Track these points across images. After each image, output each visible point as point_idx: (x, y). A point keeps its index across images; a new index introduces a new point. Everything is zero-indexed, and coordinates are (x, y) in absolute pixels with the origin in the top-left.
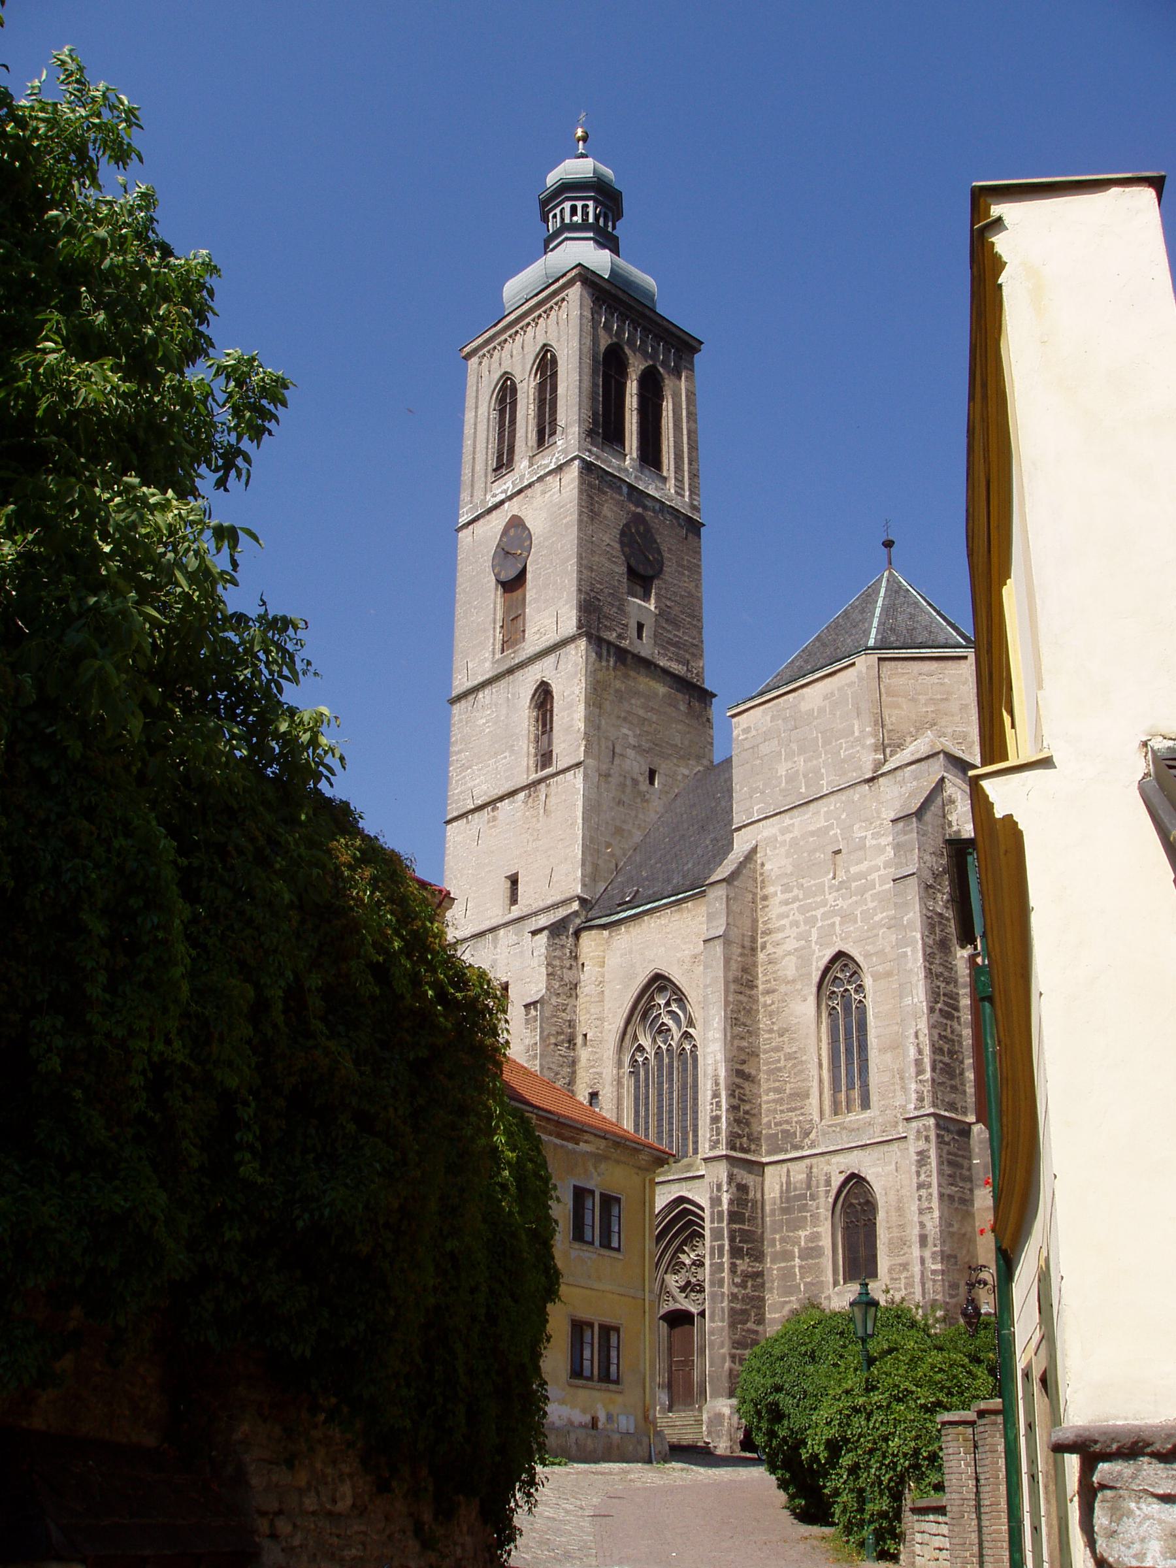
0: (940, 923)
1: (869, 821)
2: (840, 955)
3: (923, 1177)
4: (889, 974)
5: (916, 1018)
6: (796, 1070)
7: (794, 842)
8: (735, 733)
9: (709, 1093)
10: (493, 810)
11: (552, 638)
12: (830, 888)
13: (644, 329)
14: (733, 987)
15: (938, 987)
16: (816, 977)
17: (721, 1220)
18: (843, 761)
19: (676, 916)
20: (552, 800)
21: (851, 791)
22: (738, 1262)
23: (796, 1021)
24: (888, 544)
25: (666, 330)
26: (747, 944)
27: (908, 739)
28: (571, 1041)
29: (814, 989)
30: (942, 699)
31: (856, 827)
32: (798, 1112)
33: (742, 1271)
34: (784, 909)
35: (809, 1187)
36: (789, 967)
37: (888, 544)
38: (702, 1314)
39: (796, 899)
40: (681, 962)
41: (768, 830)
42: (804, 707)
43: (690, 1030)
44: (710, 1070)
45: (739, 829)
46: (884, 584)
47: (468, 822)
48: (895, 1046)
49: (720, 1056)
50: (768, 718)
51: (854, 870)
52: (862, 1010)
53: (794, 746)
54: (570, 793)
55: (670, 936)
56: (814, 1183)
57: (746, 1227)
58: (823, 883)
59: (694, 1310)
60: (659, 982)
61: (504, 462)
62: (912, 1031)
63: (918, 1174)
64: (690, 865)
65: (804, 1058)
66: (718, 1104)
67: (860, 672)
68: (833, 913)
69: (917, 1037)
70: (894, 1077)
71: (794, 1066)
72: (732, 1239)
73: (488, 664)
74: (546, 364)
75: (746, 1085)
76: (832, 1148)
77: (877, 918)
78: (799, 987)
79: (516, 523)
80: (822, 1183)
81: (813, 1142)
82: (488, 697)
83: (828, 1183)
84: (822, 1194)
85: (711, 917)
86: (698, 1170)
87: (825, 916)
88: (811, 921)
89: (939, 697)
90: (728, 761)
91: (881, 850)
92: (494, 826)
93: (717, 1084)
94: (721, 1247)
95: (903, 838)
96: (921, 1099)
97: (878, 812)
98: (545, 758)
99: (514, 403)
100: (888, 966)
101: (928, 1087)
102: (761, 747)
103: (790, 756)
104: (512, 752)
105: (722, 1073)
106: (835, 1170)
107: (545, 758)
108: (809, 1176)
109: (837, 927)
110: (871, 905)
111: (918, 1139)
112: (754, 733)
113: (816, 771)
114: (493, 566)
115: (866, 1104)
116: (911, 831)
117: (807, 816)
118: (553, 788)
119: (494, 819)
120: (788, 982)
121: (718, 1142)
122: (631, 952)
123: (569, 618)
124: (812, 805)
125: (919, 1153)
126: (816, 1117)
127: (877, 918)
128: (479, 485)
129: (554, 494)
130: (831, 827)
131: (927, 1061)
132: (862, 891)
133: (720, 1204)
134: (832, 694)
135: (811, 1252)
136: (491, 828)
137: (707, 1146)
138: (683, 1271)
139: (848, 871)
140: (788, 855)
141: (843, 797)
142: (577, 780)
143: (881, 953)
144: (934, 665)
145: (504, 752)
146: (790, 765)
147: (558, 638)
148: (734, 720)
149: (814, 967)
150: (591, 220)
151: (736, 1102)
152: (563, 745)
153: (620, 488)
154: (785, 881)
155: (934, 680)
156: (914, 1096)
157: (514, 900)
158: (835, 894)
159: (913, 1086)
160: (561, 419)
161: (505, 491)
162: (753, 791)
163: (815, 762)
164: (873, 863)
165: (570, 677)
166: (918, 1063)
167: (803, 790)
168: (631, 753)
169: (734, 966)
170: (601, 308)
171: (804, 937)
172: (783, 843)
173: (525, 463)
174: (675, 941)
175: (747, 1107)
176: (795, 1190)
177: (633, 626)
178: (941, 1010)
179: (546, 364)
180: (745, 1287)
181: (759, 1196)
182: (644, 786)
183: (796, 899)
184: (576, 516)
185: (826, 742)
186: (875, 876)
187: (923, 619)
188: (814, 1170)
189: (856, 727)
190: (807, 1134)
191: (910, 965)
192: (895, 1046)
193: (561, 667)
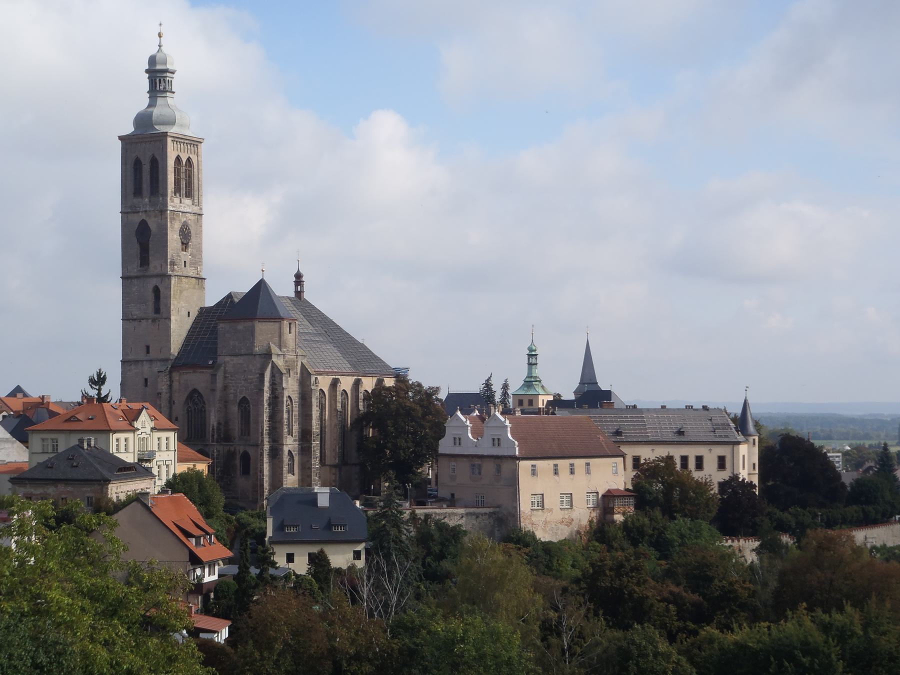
2: (244, 397)
36: (231, 397)
41: (228, 359)
60: (195, 391)
98: (157, 310)
105: (215, 424)
106: (241, 449)
107: (157, 310)
115: (249, 434)
173: (147, 200)
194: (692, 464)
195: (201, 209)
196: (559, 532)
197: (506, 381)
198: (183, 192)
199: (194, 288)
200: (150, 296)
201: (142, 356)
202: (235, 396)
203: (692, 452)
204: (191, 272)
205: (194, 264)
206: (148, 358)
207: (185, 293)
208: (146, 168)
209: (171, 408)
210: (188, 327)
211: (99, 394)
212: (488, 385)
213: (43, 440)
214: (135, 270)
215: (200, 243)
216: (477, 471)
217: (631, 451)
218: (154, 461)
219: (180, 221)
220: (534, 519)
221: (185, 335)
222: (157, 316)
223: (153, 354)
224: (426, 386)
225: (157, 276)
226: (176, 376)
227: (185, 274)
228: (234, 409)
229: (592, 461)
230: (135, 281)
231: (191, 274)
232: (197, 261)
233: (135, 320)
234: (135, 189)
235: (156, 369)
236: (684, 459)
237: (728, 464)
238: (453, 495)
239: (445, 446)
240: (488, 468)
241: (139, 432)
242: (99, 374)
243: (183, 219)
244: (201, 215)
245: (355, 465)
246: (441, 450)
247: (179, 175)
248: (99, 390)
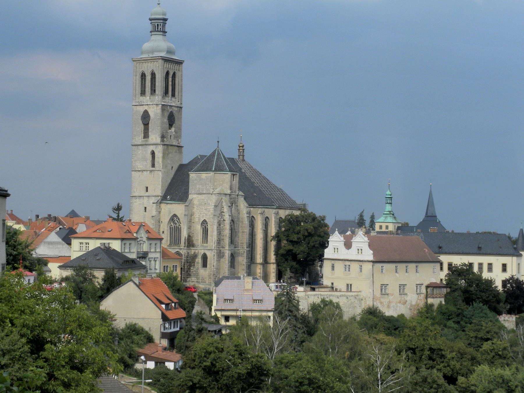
24: (218, 142)
28: (159, 222)
36: (197, 220)
37: (218, 142)
41: (195, 196)
48: (212, 236)
52: (208, 229)
60: (175, 215)
88: (201, 213)
98: (153, 165)
99: (145, 79)
105: (186, 236)
106: (202, 252)
107: (153, 165)
128: (137, 96)
135: (198, 263)
142: (160, 173)
165: (159, 152)
173: (148, 98)
174: (178, 209)
177: (169, 137)
187: (222, 162)
194: (485, 268)
195: (181, 104)
196: (398, 308)
197: (373, 214)
199: (176, 152)
200: (150, 157)
201: (143, 193)
202: (199, 219)
203: (485, 260)
204: (175, 143)
205: (177, 137)
206: (147, 194)
207: (170, 155)
208: (148, 78)
209: (160, 226)
210: (172, 176)
211: (118, 216)
212: (361, 216)
213: (81, 243)
214: (139, 139)
215: (181, 125)
216: (347, 269)
217: (446, 259)
218: (147, 258)
219: (168, 111)
220: (382, 300)
221: (170, 181)
222: (153, 169)
223: (150, 193)
224: (317, 215)
225: (153, 145)
226: (163, 205)
227: (171, 143)
228: (198, 229)
229: (420, 265)
230: (140, 147)
231: (174, 143)
232: (178, 136)
234: (142, 91)
235: (152, 202)
236: (481, 265)
237: (508, 268)
238: (332, 284)
239: (328, 253)
240: (355, 267)
241: (139, 240)
242: (119, 204)
243: (170, 110)
244: (181, 108)
245: (273, 263)
246: (326, 256)
247: (168, 83)
248: (118, 214)
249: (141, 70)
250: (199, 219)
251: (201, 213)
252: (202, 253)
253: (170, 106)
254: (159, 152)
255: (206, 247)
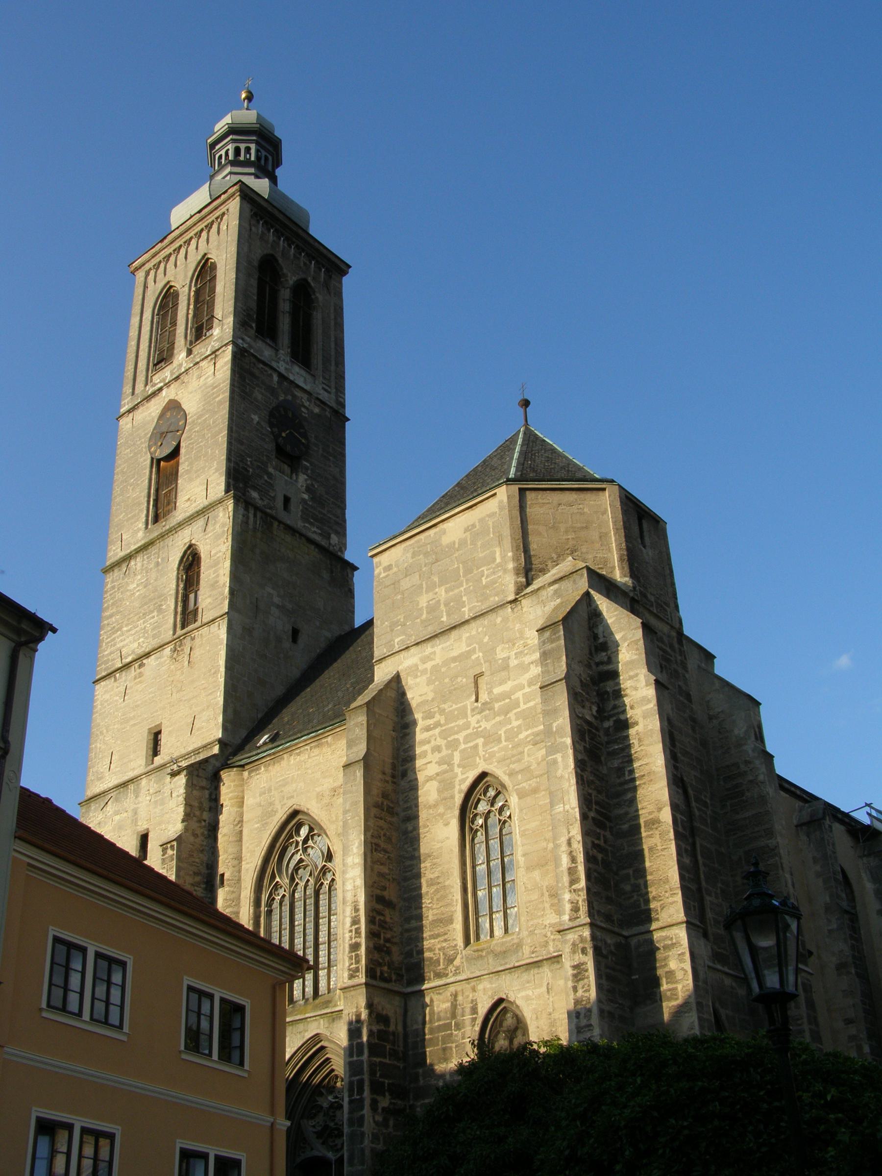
0: (589, 731)
1: (512, 642)
2: (484, 775)
3: (580, 993)
4: (535, 791)
5: (568, 824)
6: (438, 896)
7: (435, 669)
8: (376, 572)
9: (348, 921)
10: (140, 666)
11: (201, 502)
12: (473, 710)
13: (297, 247)
14: (374, 811)
15: (590, 795)
16: (459, 799)
17: (360, 1053)
18: (486, 587)
19: (316, 751)
20: (196, 653)
21: (491, 617)
22: (379, 1098)
23: (439, 845)
25: (317, 250)
26: (388, 770)
27: (550, 564)
29: (457, 812)
30: (583, 528)
31: (498, 649)
32: (441, 939)
33: (384, 1109)
34: (426, 735)
35: (454, 1015)
37: (526, 403)
38: (340, 1161)
39: (437, 724)
40: (320, 796)
42: (446, 540)
43: (329, 865)
44: (349, 896)
45: (380, 660)
46: (521, 436)
47: (115, 680)
49: (360, 882)
50: (409, 555)
51: (497, 690)
53: (436, 579)
54: (213, 642)
55: (310, 771)
56: (459, 1011)
57: (387, 1061)
58: (465, 707)
59: (331, 1155)
61: (162, 357)
62: (563, 840)
63: (575, 989)
64: (330, 706)
65: (447, 883)
66: (358, 932)
67: (501, 502)
68: (477, 734)
69: (569, 843)
70: (542, 895)
71: (437, 891)
72: (372, 1073)
73: (141, 534)
74: (205, 271)
75: (387, 912)
76: (478, 973)
77: (521, 736)
78: (441, 810)
79: (174, 406)
80: (468, 1010)
81: (458, 968)
82: (139, 565)
83: (474, 1010)
84: (468, 1022)
85: (350, 744)
86: (336, 1005)
87: (467, 739)
89: (579, 525)
90: (370, 624)
91: (523, 668)
92: (140, 682)
93: (356, 910)
94: (361, 1083)
95: (549, 646)
96: (576, 909)
97: (521, 632)
100: (533, 783)
101: (583, 895)
102: (402, 583)
103: (431, 587)
104: (160, 610)
108: (454, 1006)
109: (480, 748)
110: (515, 723)
111: (574, 952)
112: (395, 569)
113: (458, 600)
114: (150, 447)
116: (558, 638)
117: (448, 643)
118: (197, 641)
119: (141, 675)
120: (430, 807)
121: (357, 970)
122: (270, 790)
123: (218, 484)
124: (454, 634)
125: (575, 967)
126: (460, 941)
127: (521, 736)
129: (208, 377)
130: (473, 651)
131: (581, 869)
132: (506, 711)
133: (360, 1035)
134: (473, 526)
136: (136, 684)
137: (346, 974)
138: (322, 1114)
139: (490, 692)
140: (429, 682)
141: (485, 621)
142: (221, 632)
143: (527, 769)
144: (573, 496)
145: (153, 612)
146: (431, 595)
147: (206, 503)
148: (376, 560)
149: (457, 787)
150: (253, 158)
151: (376, 928)
152: (209, 600)
153: (271, 375)
154: (427, 708)
155: (574, 509)
156: (568, 907)
157: (155, 752)
158: (478, 717)
159: (567, 896)
160: (218, 313)
161: (164, 380)
162: (393, 625)
163: (456, 591)
164: (515, 683)
166: (572, 871)
167: (444, 619)
168: (274, 610)
169: (375, 792)
170: (258, 222)
171: (447, 761)
172: (424, 671)
173: (184, 354)
174: (313, 777)
175: (388, 936)
176: (439, 1020)
178: (593, 819)
179: (205, 271)
180: (386, 1126)
181: (400, 1028)
182: (287, 644)
183: (437, 724)
184: (227, 394)
185: (468, 571)
186: (519, 695)
188: (460, 998)
189: (498, 554)
190: (451, 961)
191: (559, 773)
192: (541, 863)
193: (210, 527)
198: (285, 339)
233: (127, 666)
249: (160, 285)
250: (446, 785)
251: (453, 745)
252: (482, 1010)
253: (282, 376)
254: (218, 537)
255: (503, 954)
